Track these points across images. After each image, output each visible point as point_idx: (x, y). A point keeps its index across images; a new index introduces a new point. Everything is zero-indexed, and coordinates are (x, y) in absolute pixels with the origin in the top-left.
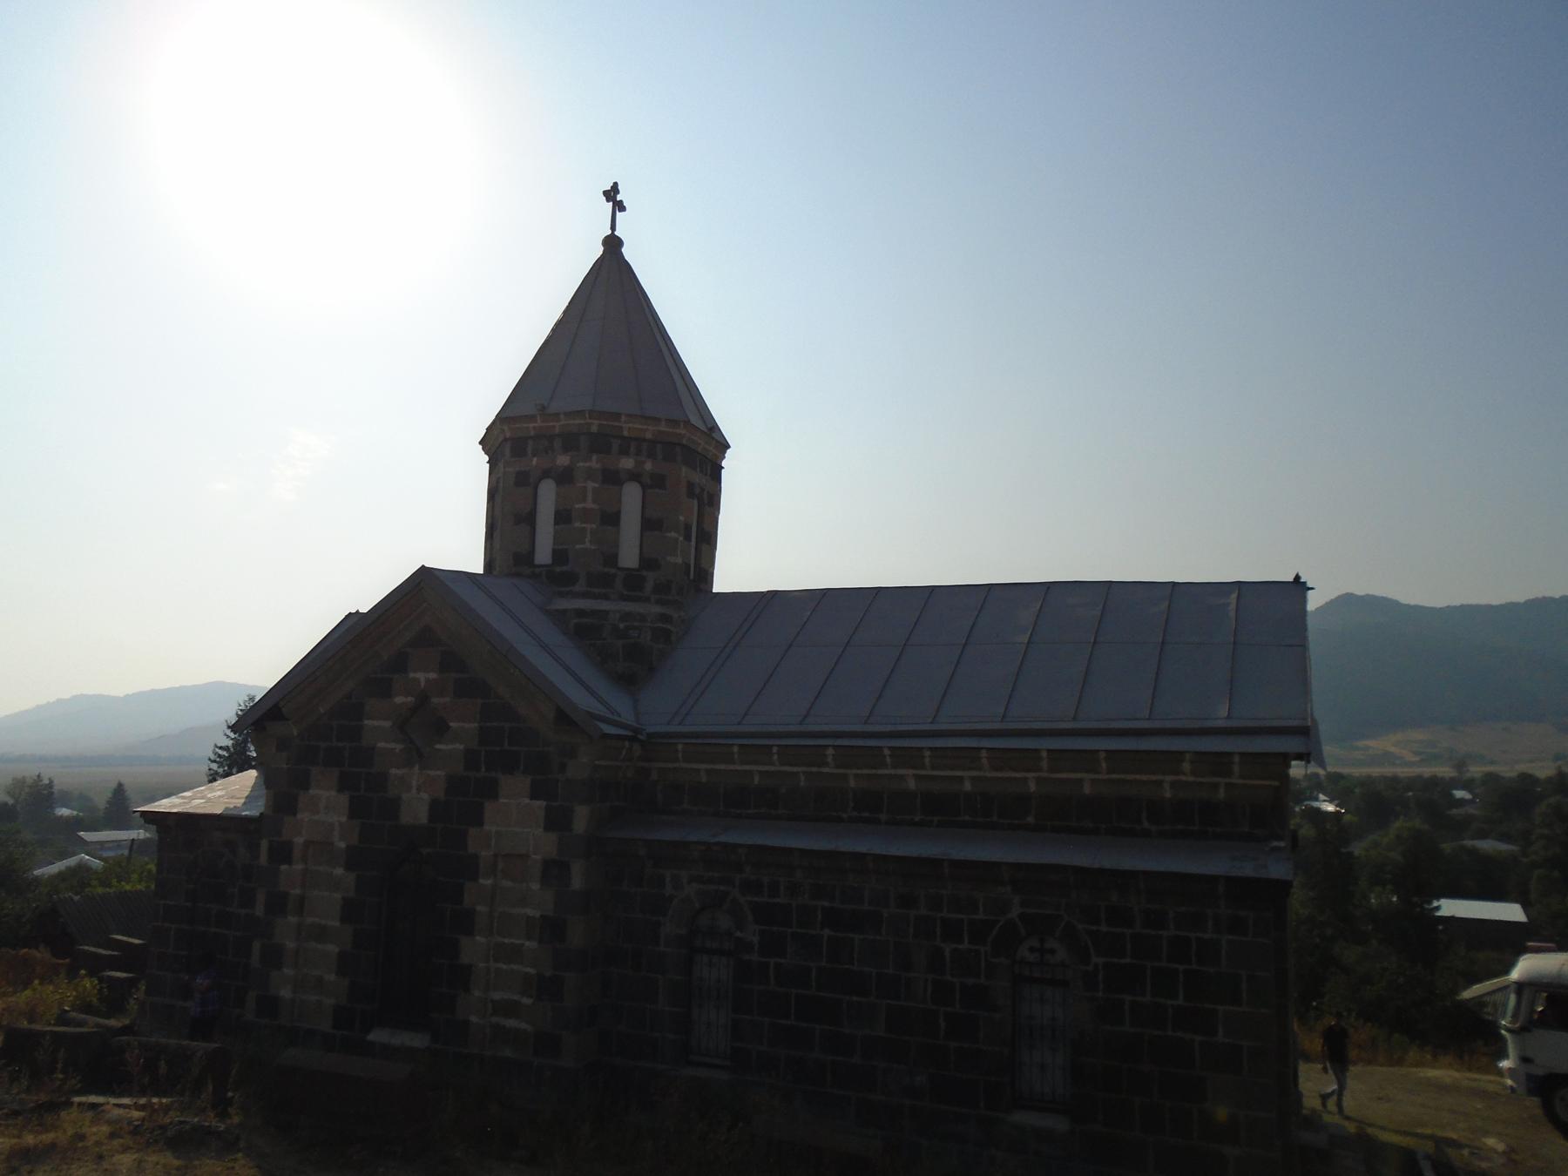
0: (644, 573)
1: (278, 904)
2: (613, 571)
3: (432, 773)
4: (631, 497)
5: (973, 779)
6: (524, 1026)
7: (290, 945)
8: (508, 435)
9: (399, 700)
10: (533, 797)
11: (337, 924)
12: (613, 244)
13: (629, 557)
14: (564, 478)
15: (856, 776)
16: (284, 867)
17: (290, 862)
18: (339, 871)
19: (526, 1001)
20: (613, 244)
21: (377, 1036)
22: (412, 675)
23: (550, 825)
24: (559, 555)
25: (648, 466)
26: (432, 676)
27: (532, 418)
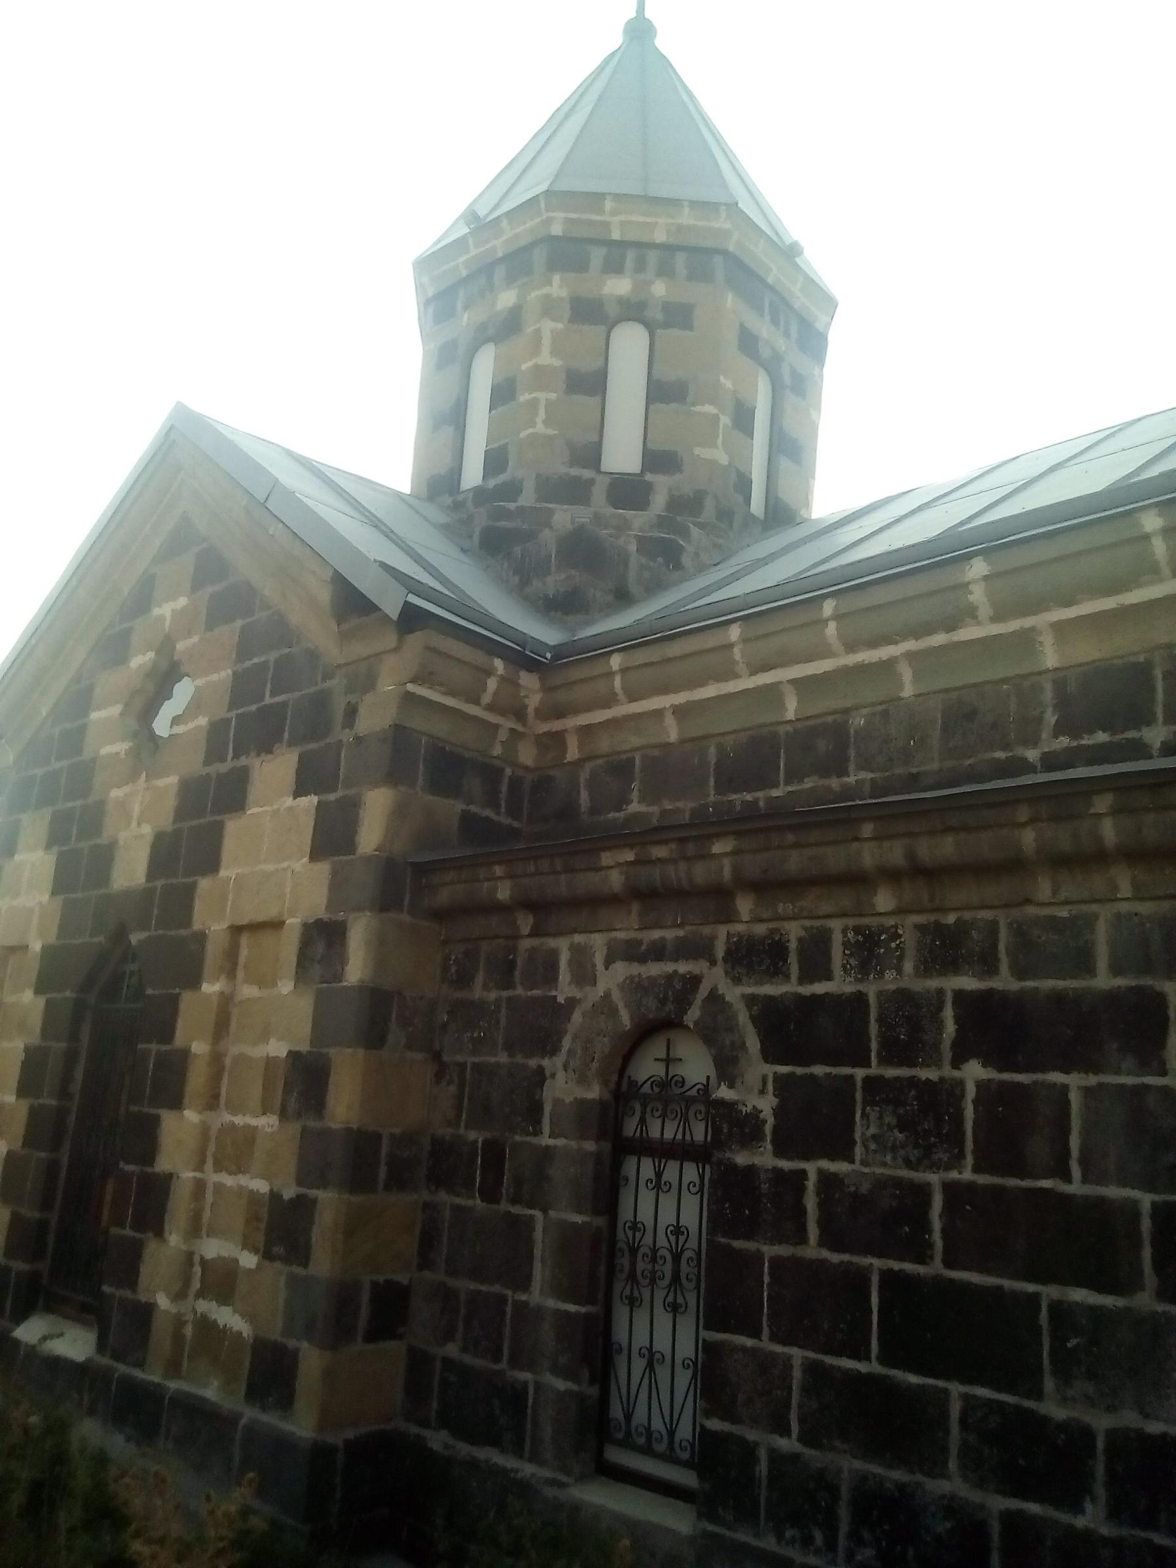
0: (649, 477)
2: (587, 474)
4: (629, 349)
12: (640, 31)
13: (623, 453)
15: (1059, 628)
20: (640, 31)
24: (495, 461)
25: (659, 289)
26: (182, 601)
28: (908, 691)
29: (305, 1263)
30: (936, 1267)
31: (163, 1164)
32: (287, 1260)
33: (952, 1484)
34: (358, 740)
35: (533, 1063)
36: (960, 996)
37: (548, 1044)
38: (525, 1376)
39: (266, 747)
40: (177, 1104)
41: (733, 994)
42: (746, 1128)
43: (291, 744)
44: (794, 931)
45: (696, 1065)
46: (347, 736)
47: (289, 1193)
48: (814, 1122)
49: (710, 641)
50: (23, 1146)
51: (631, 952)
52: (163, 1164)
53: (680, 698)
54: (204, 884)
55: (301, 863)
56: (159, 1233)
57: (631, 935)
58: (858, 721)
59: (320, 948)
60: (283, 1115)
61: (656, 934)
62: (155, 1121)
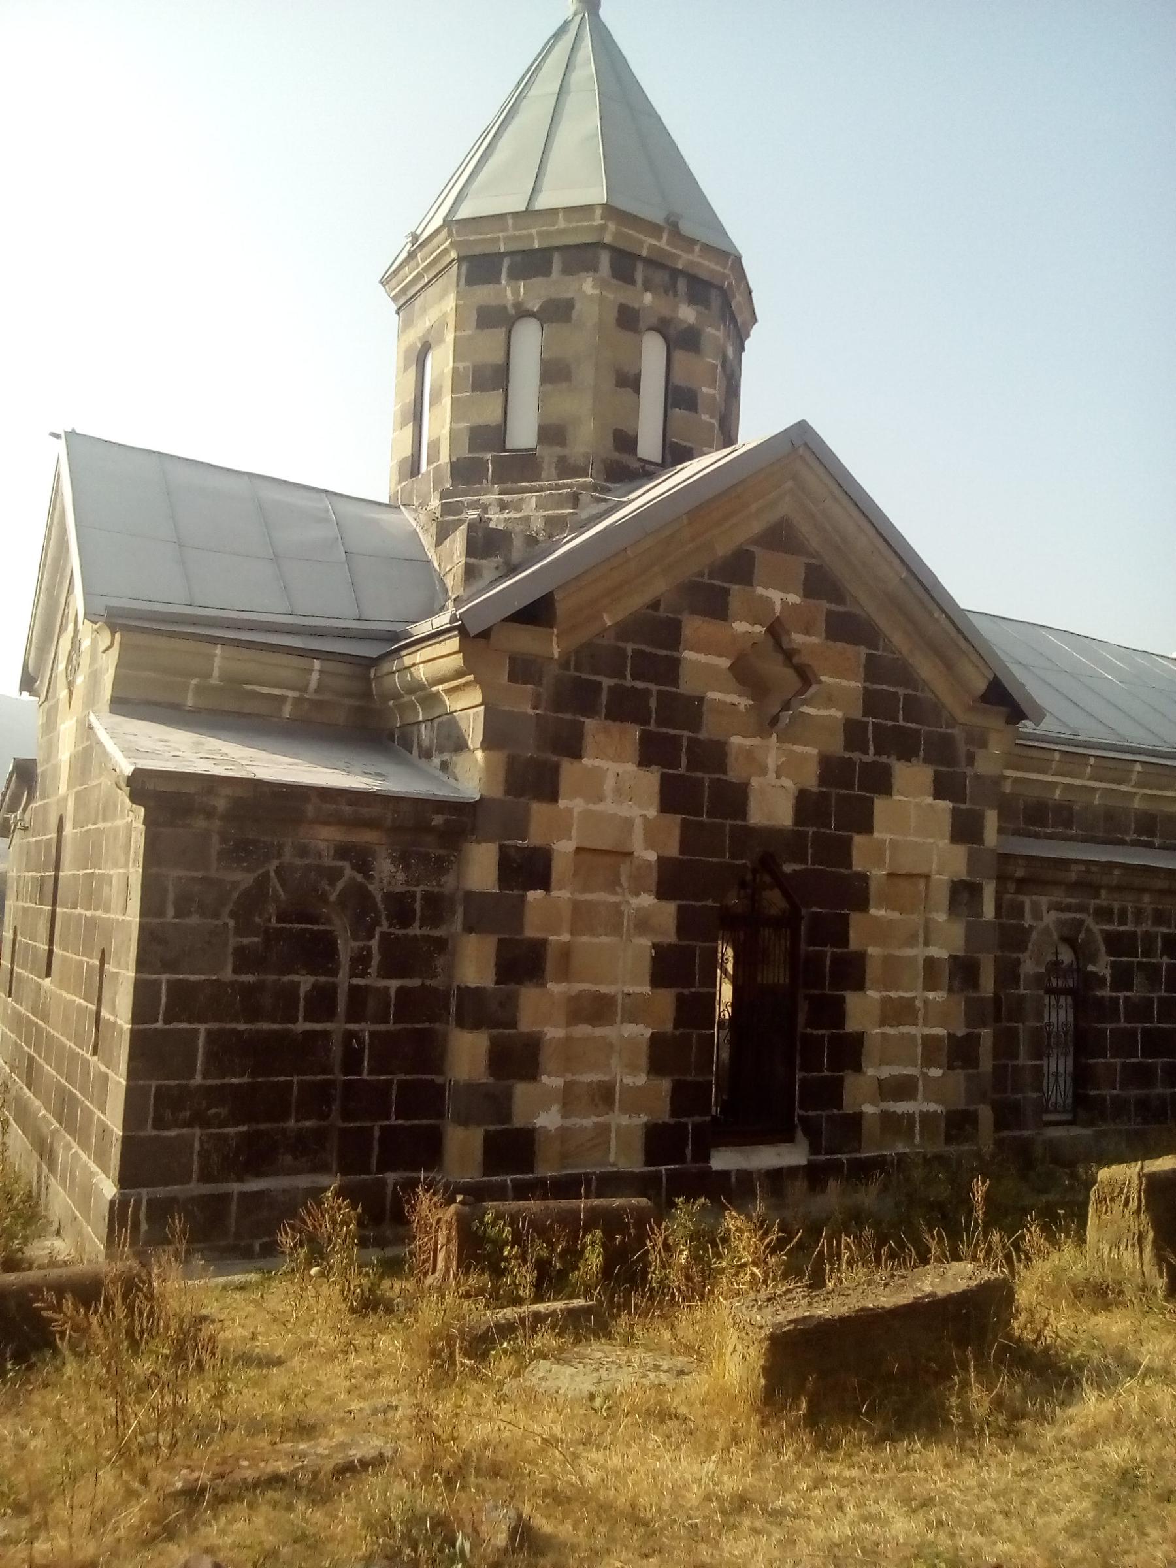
1: (523, 963)
3: (798, 749)
6: (932, 1107)
7: (554, 1033)
8: (608, 239)
9: (741, 627)
10: (937, 796)
11: (647, 989)
14: (682, 341)
16: (534, 895)
18: (647, 900)
19: (935, 1072)
21: (723, 1160)
22: (760, 590)
26: (794, 599)
27: (654, 229)
28: (1096, 802)
29: (977, 1066)
30: (1156, 1025)
31: (852, 1025)
32: (962, 1068)
33: (1159, 1090)
34: (977, 777)
35: (1014, 955)
36: (1163, 934)
37: (1021, 946)
38: (1019, 1096)
39: (907, 755)
40: (860, 986)
41: (1096, 928)
42: (1101, 981)
43: (926, 761)
44: (1116, 906)
45: (1066, 956)
46: (970, 772)
47: (961, 1032)
48: (1122, 979)
49: (1047, 755)
50: (675, 1028)
51: (1060, 908)
52: (852, 1025)
54: (858, 839)
55: (944, 843)
56: (858, 1068)
57: (1059, 899)
58: (1077, 807)
59: (965, 896)
60: (950, 990)
61: (1069, 900)
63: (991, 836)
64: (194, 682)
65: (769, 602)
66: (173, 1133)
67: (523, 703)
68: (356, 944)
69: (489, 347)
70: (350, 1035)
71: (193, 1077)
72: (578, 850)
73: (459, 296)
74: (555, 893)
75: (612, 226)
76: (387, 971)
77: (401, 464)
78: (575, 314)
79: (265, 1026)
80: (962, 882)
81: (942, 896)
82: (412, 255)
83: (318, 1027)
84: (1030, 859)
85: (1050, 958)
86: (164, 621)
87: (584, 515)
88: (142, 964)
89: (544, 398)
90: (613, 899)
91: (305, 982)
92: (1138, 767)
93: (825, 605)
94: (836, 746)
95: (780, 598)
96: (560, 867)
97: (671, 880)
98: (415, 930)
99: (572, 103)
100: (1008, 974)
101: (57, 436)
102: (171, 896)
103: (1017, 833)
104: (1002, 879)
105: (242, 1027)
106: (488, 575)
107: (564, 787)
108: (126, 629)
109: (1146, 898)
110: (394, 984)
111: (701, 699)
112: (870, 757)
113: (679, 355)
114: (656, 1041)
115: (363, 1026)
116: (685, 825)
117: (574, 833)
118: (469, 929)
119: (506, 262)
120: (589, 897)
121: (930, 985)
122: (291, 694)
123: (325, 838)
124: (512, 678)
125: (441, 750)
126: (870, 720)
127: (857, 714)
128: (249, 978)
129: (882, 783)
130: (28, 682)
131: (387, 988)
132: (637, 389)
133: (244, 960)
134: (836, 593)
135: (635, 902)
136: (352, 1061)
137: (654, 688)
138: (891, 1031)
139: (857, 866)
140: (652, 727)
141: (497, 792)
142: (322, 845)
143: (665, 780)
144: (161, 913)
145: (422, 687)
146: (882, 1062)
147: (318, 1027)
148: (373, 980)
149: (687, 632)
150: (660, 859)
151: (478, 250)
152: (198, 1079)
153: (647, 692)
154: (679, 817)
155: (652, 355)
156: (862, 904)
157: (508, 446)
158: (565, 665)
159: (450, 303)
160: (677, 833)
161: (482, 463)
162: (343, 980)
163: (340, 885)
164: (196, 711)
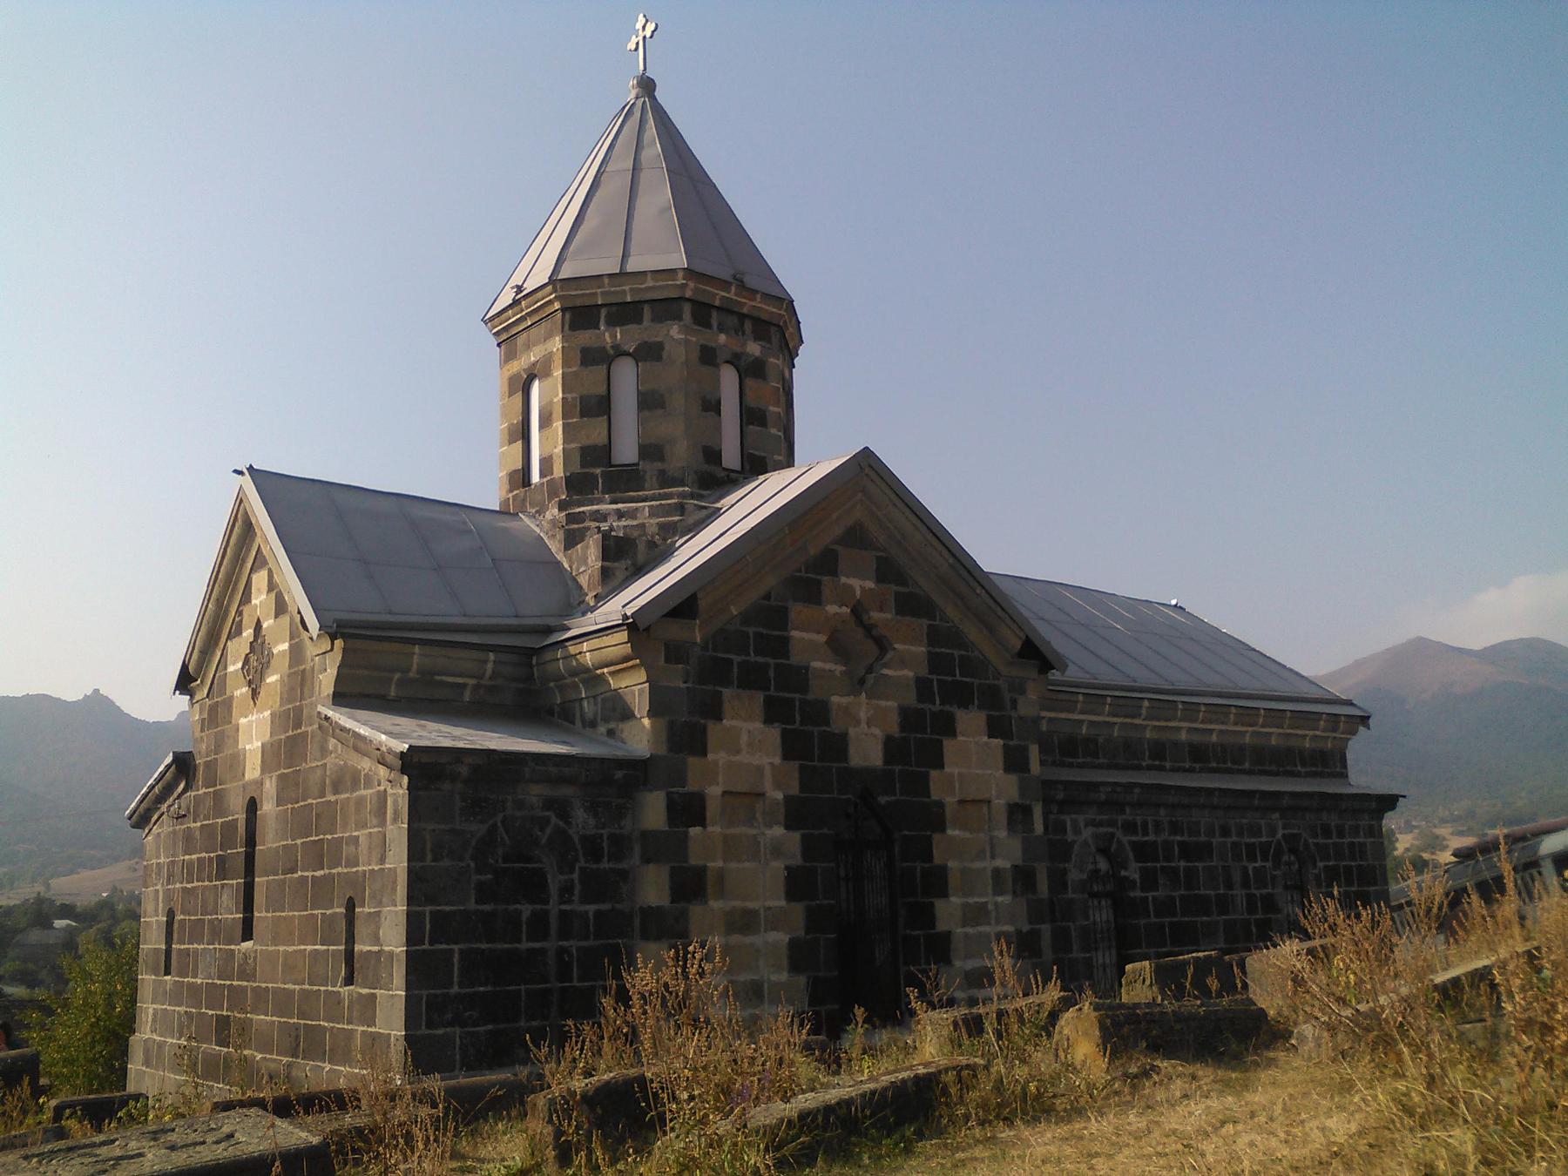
1: (691, 885)
3: (883, 703)
5: (1221, 731)
8: (688, 294)
9: (832, 609)
11: (783, 903)
12: (647, 86)
14: (751, 370)
16: (694, 831)
17: (703, 825)
18: (779, 831)
20: (647, 86)
22: (843, 579)
23: (1008, 769)
26: (870, 584)
27: (725, 285)
31: (941, 927)
34: (1021, 718)
39: (965, 704)
40: (944, 894)
43: (980, 707)
44: (1139, 820)
45: (1103, 865)
46: (1013, 714)
47: (1026, 928)
49: (1073, 698)
51: (1091, 823)
52: (941, 927)
53: (1053, 715)
54: (934, 774)
58: (1101, 740)
62: (932, 904)
63: (1035, 767)
64: (397, 676)
65: (850, 588)
66: (440, 1032)
67: (676, 679)
68: (562, 877)
69: (593, 381)
70: (562, 951)
71: (451, 985)
72: (725, 793)
73: (564, 339)
74: (710, 829)
75: (691, 284)
76: (586, 899)
77: (512, 475)
78: (665, 355)
79: (499, 946)
80: (1016, 805)
81: (1002, 817)
82: (516, 302)
83: (537, 945)
84: (1067, 785)
85: (1090, 867)
86: (377, 628)
87: (691, 521)
88: (410, 900)
89: (641, 422)
90: (753, 832)
91: (526, 910)
92: (1146, 703)
93: (894, 588)
94: (911, 698)
95: (860, 585)
96: (712, 808)
97: (795, 814)
98: (605, 865)
99: (644, 177)
100: (1058, 881)
101: (236, 471)
102: (429, 846)
103: (1054, 763)
104: (1047, 801)
105: (483, 946)
106: (620, 575)
107: (712, 742)
108: (344, 637)
109: (1162, 812)
110: (592, 908)
111: (807, 668)
112: (937, 707)
113: (749, 382)
114: (793, 945)
115: (572, 942)
116: (802, 769)
117: (720, 779)
118: (647, 860)
119: (603, 312)
120: (733, 831)
121: (998, 889)
122: (472, 682)
123: (535, 793)
124: (667, 660)
125: (606, 720)
126: (934, 677)
127: (924, 672)
128: (487, 908)
129: (948, 727)
130: (185, 682)
131: (587, 912)
132: (719, 414)
133: (484, 893)
134: (901, 580)
135: (769, 832)
136: (564, 974)
137: (771, 661)
138: (970, 930)
139: (936, 793)
140: (772, 692)
141: (662, 751)
142: (534, 800)
143: (785, 735)
144: (423, 859)
145: (587, 670)
146: (967, 957)
147: (537, 945)
148: (576, 906)
149: (792, 615)
150: (788, 799)
151: (579, 303)
152: (455, 989)
153: (767, 665)
154: (797, 764)
155: (728, 380)
156: (941, 827)
157: (614, 462)
158: (705, 647)
159: (556, 344)
160: (796, 775)
161: (595, 477)
162: (554, 907)
163: (548, 831)
164: (398, 700)
